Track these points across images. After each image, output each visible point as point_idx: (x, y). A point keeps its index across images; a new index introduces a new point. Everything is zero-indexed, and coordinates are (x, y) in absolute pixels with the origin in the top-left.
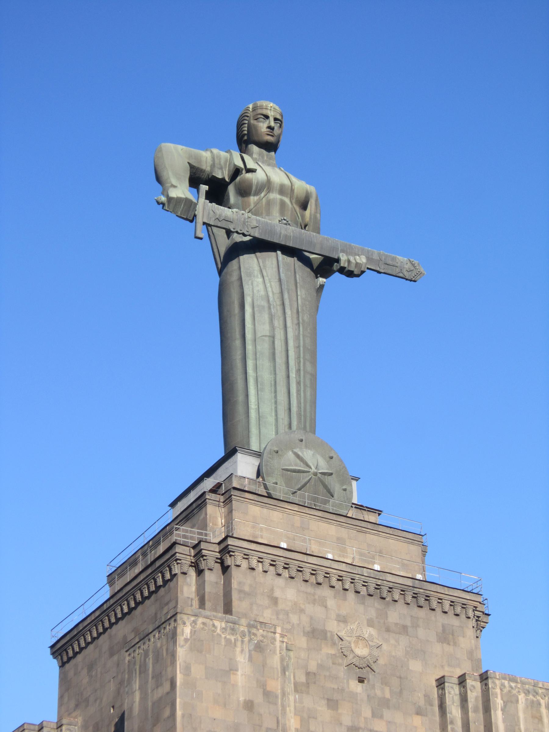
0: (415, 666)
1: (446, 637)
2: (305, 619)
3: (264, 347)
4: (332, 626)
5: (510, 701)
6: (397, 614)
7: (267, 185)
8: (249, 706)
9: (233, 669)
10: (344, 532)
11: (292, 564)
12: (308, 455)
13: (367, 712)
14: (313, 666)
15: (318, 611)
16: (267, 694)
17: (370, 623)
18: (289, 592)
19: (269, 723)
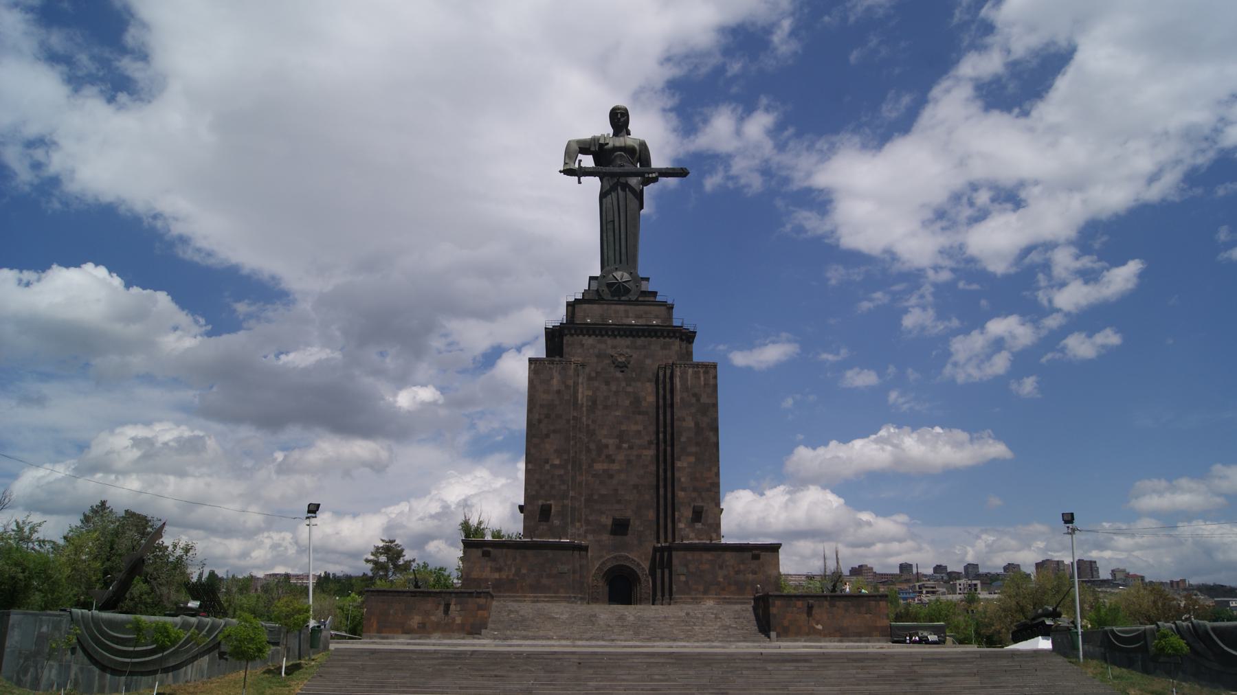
0: (648, 361)
1: (664, 347)
2: (596, 351)
3: (610, 226)
4: (610, 352)
5: (684, 373)
6: (640, 341)
7: (615, 149)
8: (559, 392)
9: (552, 378)
10: (628, 307)
12: (618, 275)
13: (624, 384)
14: (599, 369)
15: (603, 346)
16: (567, 387)
17: (628, 347)
18: (589, 341)
19: (567, 397)
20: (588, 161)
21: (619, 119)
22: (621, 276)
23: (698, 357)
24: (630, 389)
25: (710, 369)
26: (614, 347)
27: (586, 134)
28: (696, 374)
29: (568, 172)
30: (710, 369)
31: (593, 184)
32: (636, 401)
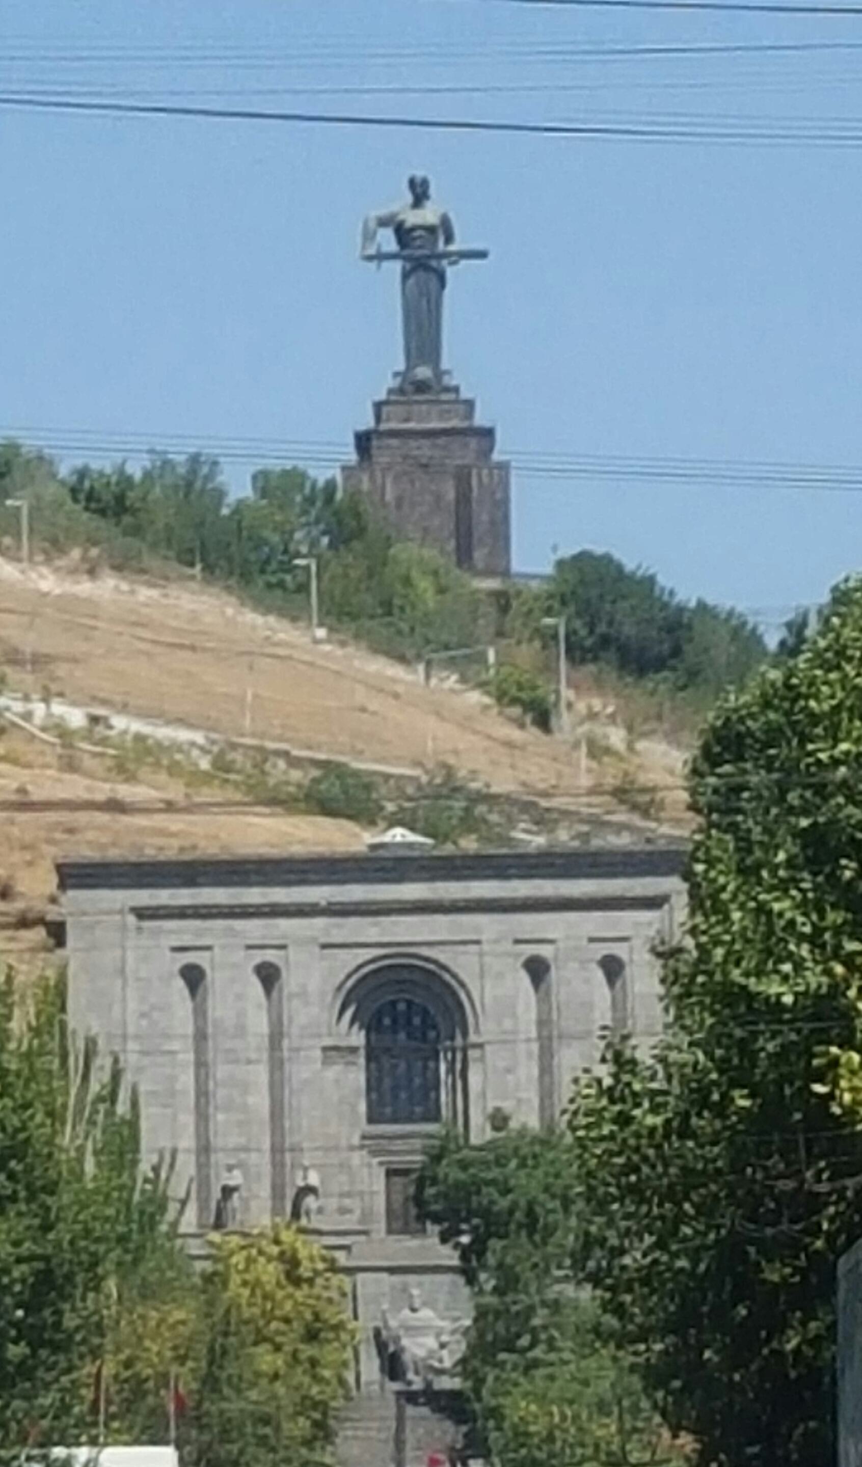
6: (441, 441)
7: (414, 229)
11: (393, 434)
18: (394, 442)
20: (387, 240)
21: (419, 192)
22: (423, 372)
23: (496, 457)
24: (433, 487)
25: (504, 467)
26: (419, 448)
27: (383, 212)
28: (491, 475)
29: (370, 258)
30: (504, 467)
31: (396, 267)
32: (438, 498)
